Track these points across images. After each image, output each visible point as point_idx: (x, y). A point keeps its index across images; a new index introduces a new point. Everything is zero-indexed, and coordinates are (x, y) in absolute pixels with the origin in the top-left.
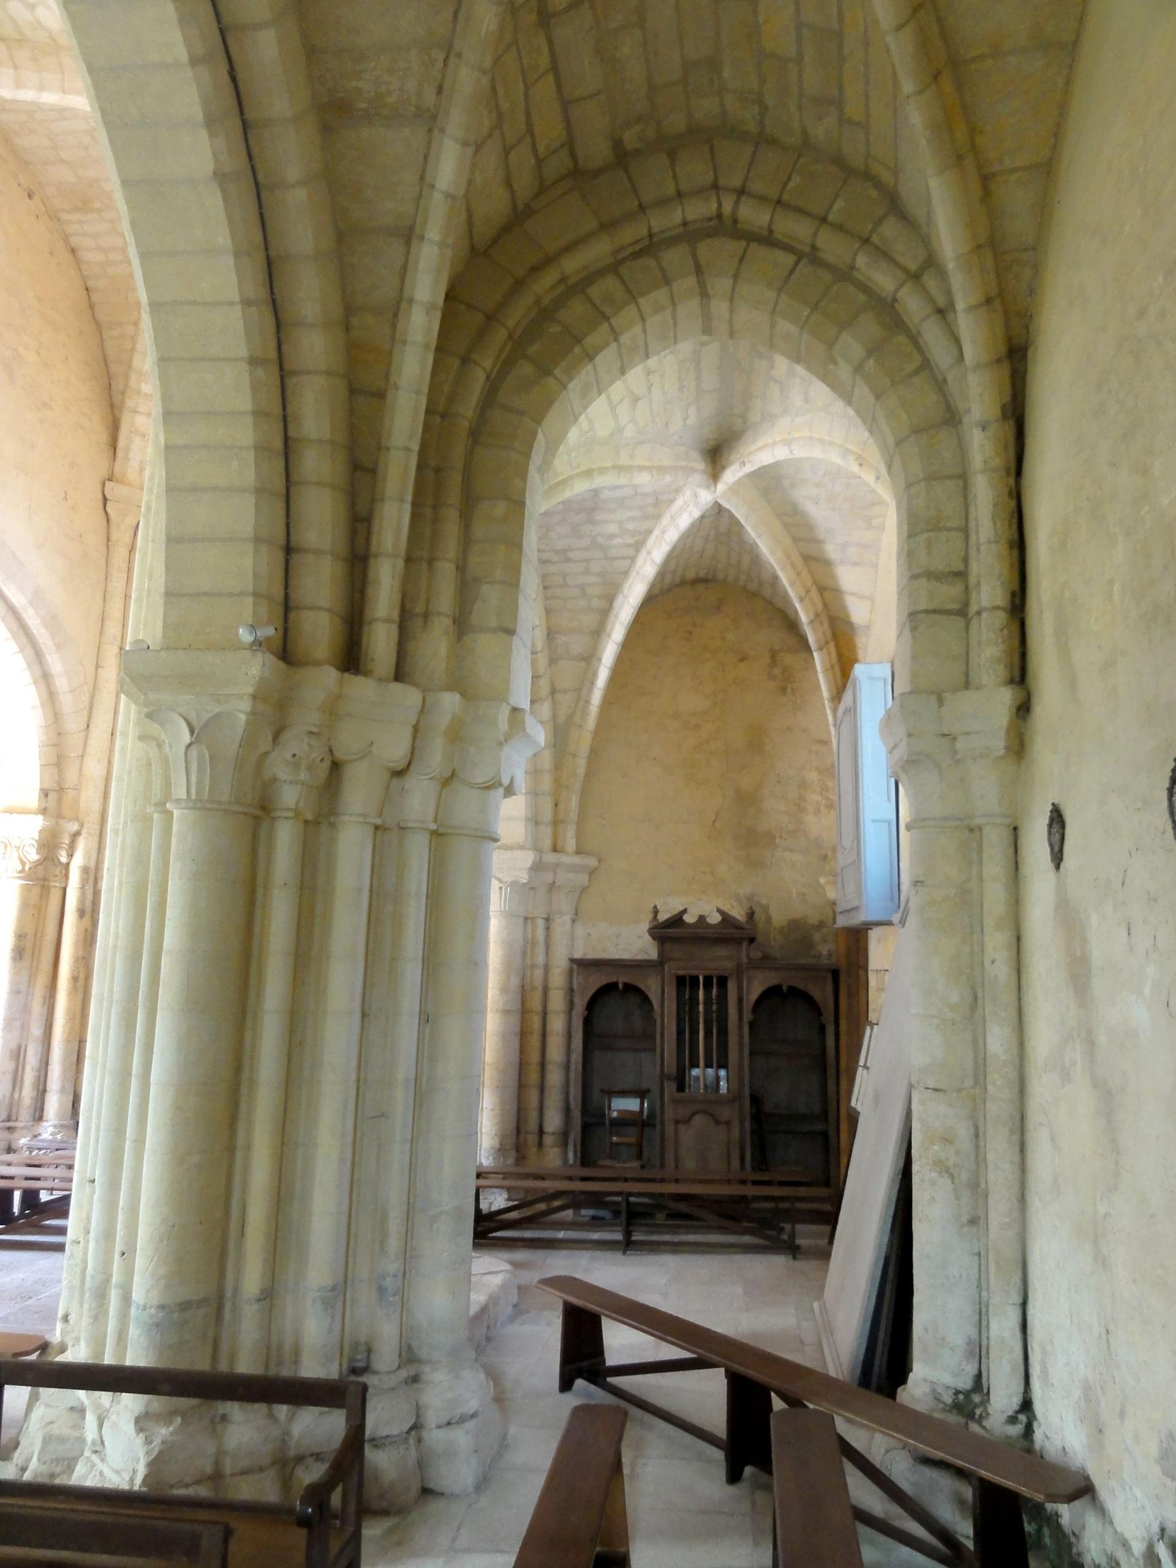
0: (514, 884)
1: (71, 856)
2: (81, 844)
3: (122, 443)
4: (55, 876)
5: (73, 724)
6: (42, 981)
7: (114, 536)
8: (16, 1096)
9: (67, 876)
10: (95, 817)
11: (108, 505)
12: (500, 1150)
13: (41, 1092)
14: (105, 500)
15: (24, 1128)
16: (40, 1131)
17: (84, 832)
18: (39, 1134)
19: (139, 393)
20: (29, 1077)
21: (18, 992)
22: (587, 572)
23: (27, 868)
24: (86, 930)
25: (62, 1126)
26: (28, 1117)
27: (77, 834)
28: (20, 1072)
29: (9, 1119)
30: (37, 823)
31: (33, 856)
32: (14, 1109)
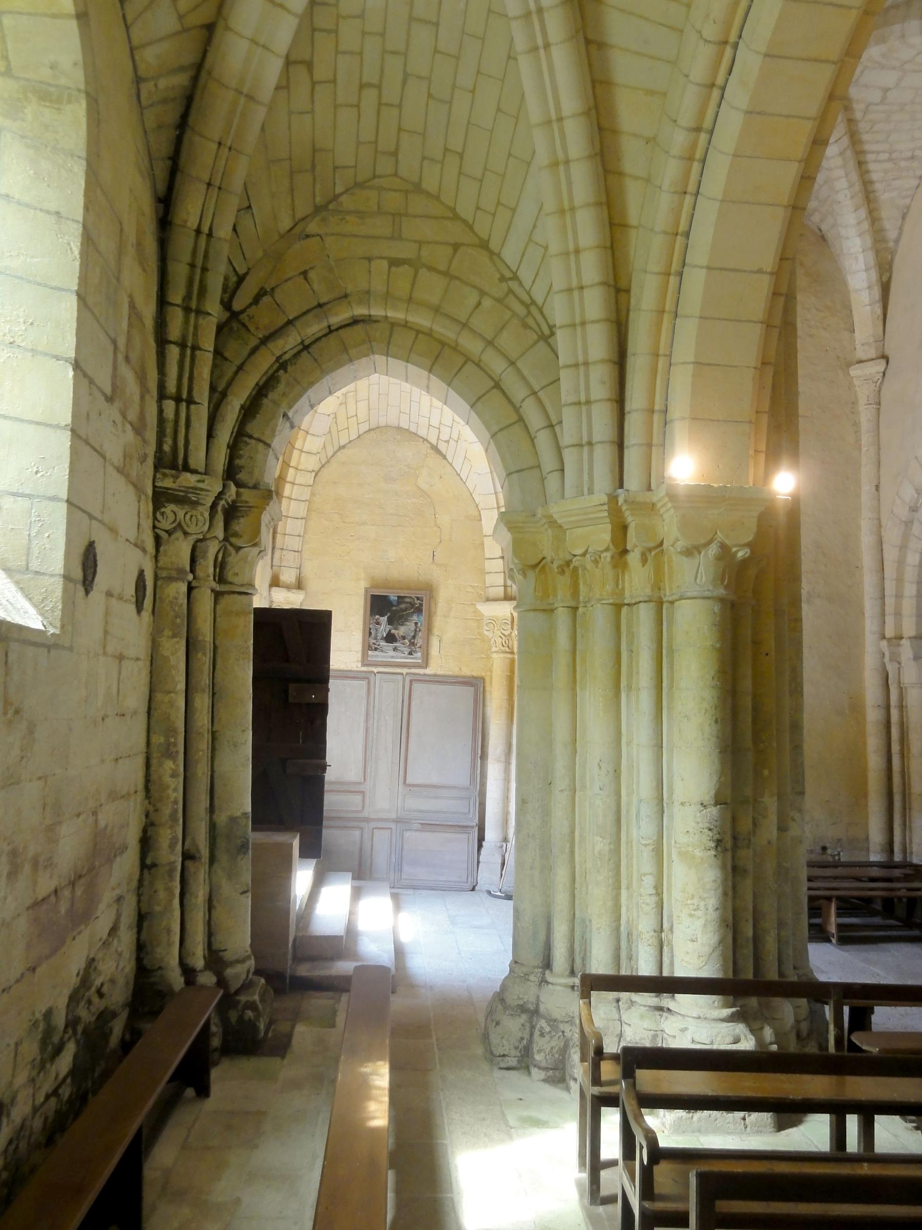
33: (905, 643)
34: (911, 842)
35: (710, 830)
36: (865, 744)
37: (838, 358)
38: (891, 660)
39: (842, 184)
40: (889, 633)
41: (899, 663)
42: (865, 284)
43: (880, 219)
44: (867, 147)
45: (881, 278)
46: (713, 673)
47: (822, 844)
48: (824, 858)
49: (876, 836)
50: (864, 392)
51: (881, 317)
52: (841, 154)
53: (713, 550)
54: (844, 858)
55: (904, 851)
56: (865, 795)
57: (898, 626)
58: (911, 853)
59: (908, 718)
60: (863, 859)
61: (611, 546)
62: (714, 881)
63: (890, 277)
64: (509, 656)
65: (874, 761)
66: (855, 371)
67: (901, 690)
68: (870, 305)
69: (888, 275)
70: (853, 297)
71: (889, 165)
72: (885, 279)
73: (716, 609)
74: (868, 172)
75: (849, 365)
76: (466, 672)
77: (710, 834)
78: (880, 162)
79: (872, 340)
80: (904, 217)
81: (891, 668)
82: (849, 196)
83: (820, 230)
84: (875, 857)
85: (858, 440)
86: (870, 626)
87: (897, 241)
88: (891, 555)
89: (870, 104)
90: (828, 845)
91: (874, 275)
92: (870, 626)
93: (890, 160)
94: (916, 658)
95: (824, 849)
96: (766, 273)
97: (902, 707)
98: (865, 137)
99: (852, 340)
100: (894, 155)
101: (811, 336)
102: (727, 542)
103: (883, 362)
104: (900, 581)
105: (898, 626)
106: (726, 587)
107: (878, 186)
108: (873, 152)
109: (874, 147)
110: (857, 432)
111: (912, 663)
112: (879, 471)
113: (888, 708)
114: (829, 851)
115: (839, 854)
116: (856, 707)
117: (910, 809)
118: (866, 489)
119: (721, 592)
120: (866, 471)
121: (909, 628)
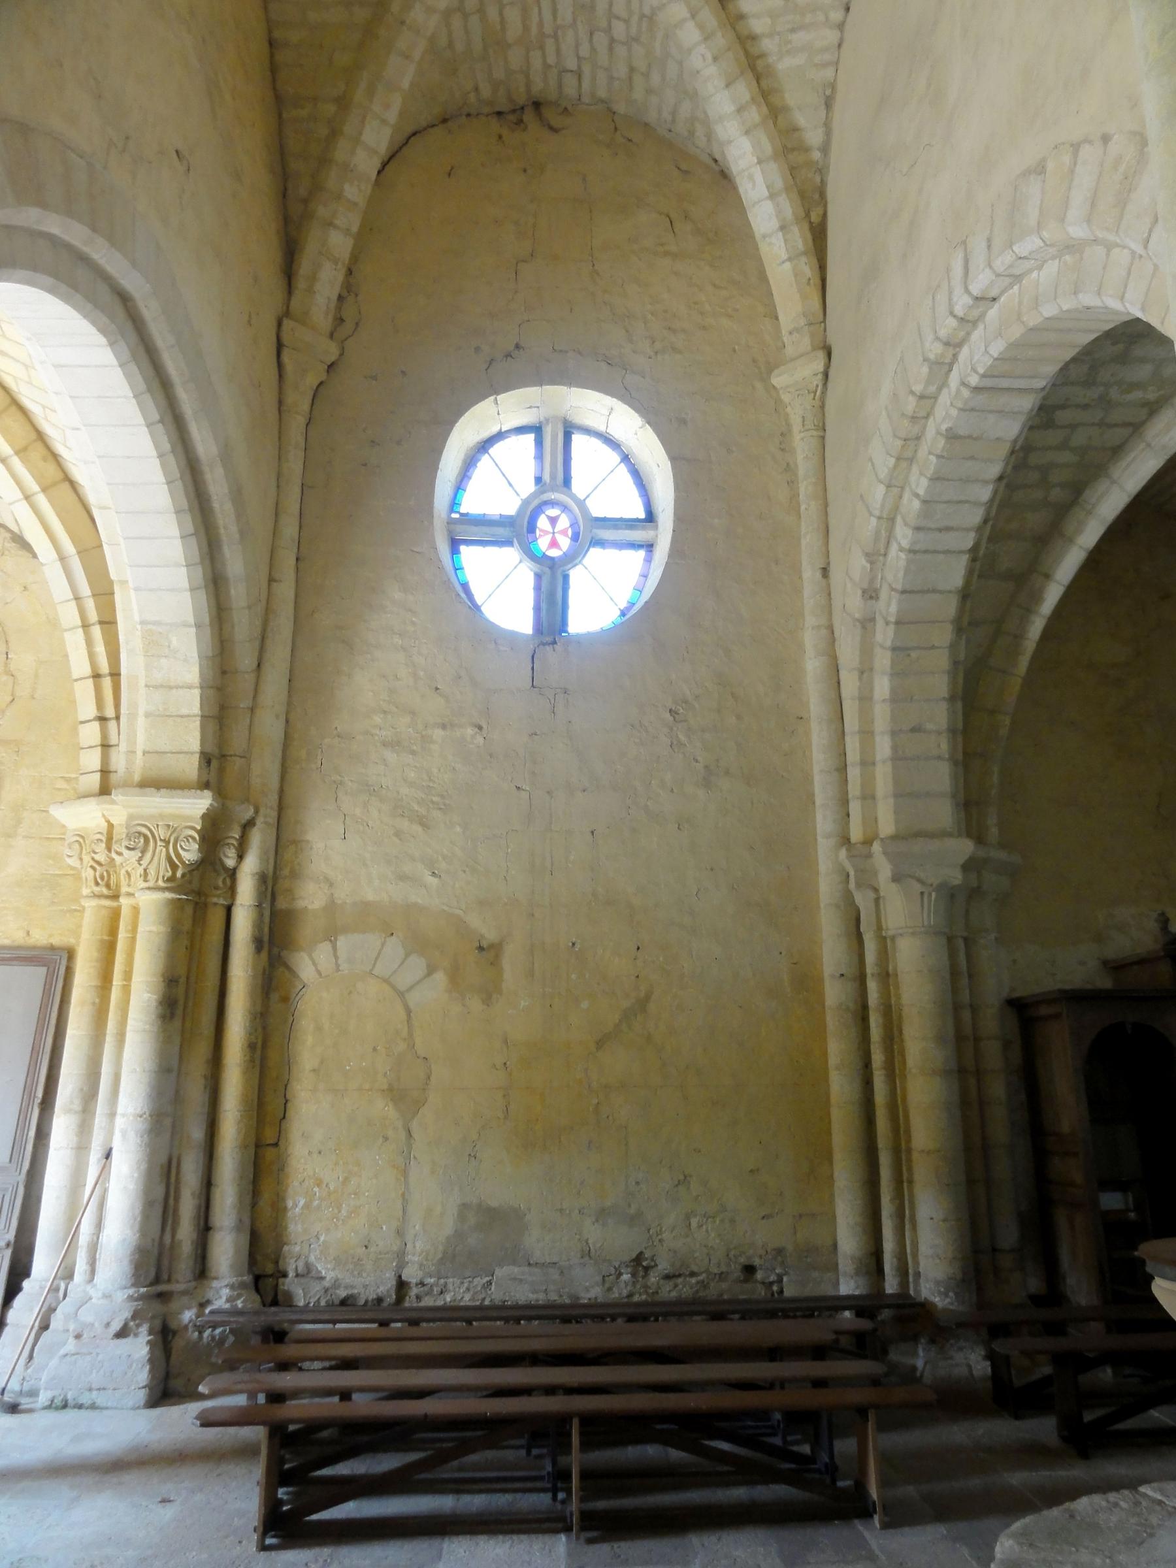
0: (942, 887)
1: (241, 857)
2: (256, 838)
3: (304, 267)
4: (217, 888)
5: (245, 660)
6: (202, 1050)
7: (291, 397)
8: (167, 1239)
9: (232, 890)
10: (273, 799)
12: (963, 1281)
13: (205, 1228)
14: (280, 346)
15: (185, 1293)
16: (210, 1295)
17: (259, 821)
18: (208, 1302)
19: (339, 196)
20: (188, 1207)
21: (169, 1070)
22: (1064, 446)
23: (179, 874)
24: (264, 970)
25: (242, 1286)
26: (189, 1275)
27: (248, 825)
28: (171, 1201)
29: (157, 1280)
30: (199, 804)
31: (191, 853)
32: (165, 1262)
33: (876, 847)
34: (915, 1255)
36: (825, 1054)
37: (754, 361)
38: (859, 885)
39: (690, 34)
40: (856, 834)
41: (876, 890)
42: (774, 224)
43: (785, 109)
45: (808, 215)
49: (849, 1242)
50: (798, 410)
51: (818, 282)
55: (903, 1271)
57: (870, 820)
58: (918, 1275)
59: (899, 997)
60: (826, 1290)
63: (825, 215)
64: (107, 903)
65: (840, 1087)
68: (790, 259)
69: (820, 211)
70: (764, 248)
72: (815, 218)
74: (741, 17)
76: (40, 937)
79: (802, 322)
80: (829, 103)
81: (863, 900)
83: (716, 161)
84: (848, 1287)
85: (794, 496)
86: (824, 822)
87: (825, 149)
88: (850, 685)
90: (757, 1262)
91: (788, 209)
92: (824, 822)
94: (896, 878)
95: (749, 1270)
97: (886, 977)
99: (778, 329)
101: (704, 328)
104: (867, 734)
105: (870, 820)
107: (768, 45)
110: (792, 483)
111: (894, 887)
112: (827, 543)
113: (861, 979)
114: (759, 1275)
115: (780, 1281)
116: (806, 981)
117: (911, 1182)
118: (809, 574)
120: (809, 540)
121: (887, 825)
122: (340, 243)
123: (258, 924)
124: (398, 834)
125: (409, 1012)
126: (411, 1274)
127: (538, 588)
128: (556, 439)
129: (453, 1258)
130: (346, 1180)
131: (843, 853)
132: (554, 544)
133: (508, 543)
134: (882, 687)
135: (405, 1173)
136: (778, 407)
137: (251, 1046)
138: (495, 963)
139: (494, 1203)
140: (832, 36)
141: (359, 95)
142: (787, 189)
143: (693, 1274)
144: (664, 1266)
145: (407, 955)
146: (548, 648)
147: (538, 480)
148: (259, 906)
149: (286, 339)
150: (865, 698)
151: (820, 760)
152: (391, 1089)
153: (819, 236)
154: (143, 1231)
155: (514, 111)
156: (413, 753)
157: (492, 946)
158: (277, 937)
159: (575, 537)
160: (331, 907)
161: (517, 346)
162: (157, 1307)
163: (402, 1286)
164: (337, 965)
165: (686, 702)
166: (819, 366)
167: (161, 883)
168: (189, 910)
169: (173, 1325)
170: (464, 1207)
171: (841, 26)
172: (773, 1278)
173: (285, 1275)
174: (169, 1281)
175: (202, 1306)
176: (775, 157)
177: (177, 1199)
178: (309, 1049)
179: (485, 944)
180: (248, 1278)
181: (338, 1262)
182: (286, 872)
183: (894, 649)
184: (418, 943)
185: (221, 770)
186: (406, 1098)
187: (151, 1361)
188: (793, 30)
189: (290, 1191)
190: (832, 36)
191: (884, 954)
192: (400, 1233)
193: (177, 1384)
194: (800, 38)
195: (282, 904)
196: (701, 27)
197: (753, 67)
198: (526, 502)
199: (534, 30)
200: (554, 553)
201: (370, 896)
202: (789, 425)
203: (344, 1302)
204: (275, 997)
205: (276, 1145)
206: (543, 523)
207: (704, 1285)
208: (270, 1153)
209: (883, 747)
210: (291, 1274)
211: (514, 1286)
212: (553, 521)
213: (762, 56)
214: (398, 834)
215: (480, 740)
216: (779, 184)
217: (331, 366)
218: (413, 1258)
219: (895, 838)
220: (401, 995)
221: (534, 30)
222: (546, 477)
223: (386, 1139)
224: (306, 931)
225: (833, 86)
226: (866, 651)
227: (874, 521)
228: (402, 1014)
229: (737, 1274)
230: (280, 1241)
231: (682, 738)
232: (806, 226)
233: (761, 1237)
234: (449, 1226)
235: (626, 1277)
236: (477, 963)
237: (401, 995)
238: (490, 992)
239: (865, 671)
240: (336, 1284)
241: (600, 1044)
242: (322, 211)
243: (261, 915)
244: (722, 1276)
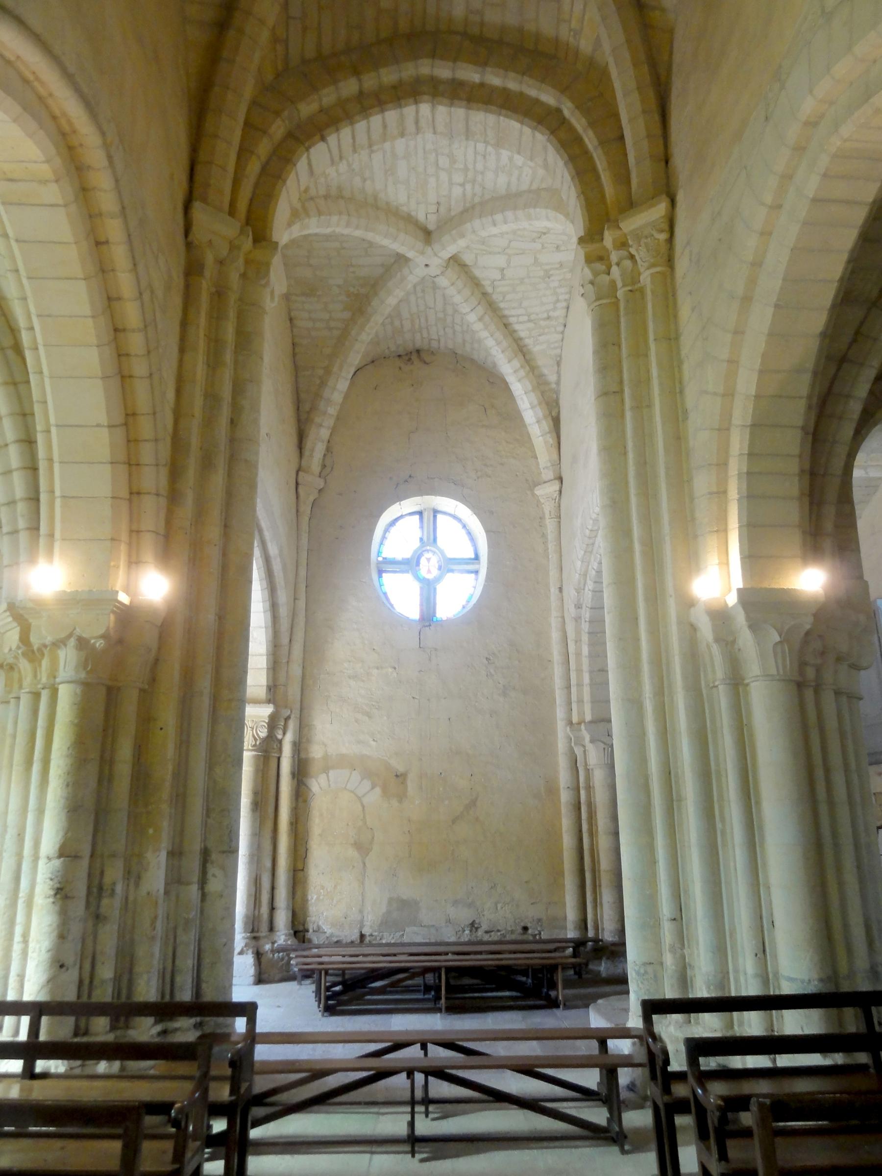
1: (284, 734)
2: (292, 725)
3: (308, 444)
5: (285, 641)
6: (269, 824)
7: (301, 509)
9: (280, 750)
10: (298, 705)
11: (300, 487)
13: (272, 909)
14: (297, 484)
15: (266, 937)
16: (276, 938)
17: (293, 716)
19: (325, 413)
23: (258, 743)
27: (287, 719)
29: (253, 931)
32: (256, 923)
35: (51, 879)
36: (561, 824)
37: (527, 480)
38: (575, 744)
40: (575, 720)
41: (584, 746)
42: (534, 420)
44: (506, 312)
45: (550, 413)
46: (68, 744)
47: (522, 924)
48: (525, 937)
49: (571, 914)
51: (556, 444)
52: (480, 319)
53: (72, 642)
54: (544, 936)
55: (596, 928)
56: (562, 874)
57: (581, 713)
58: (603, 929)
60: (561, 936)
61: (21, 645)
62: (50, 925)
65: (568, 841)
66: (539, 491)
67: (587, 771)
68: (542, 436)
69: (556, 410)
71: (531, 325)
72: (554, 414)
73: (78, 691)
74: (515, 331)
75: (536, 484)
77: (51, 883)
78: (521, 323)
79: (549, 464)
80: (558, 364)
81: (578, 751)
82: (500, 351)
85: (546, 550)
86: (560, 713)
87: (558, 383)
89: (494, 280)
90: (529, 925)
92: (560, 713)
93: (530, 321)
94: (592, 741)
95: (525, 929)
96: (104, 426)
97: (589, 788)
98: (502, 305)
99: (538, 464)
100: (533, 317)
101: (502, 464)
102: (84, 635)
103: (557, 482)
104: (579, 671)
105: (581, 713)
106: (88, 673)
107: (528, 341)
108: (513, 316)
109: (513, 312)
110: (545, 543)
111: (591, 745)
114: (530, 931)
115: (540, 934)
116: (552, 790)
117: (600, 886)
118: (554, 590)
119: (83, 675)
120: (553, 573)
122: (325, 433)
123: (293, 766)
124: (357, 721)
125: (363, 807)
126: (366, 931)
127: (421, 595)
128: (428, 518)
129: (386, 923)
130: (335, 887)
131: (568, 728)
132: (429, 571)
133: (407, 572)
134: (585, 650)
135: (363, 883)
136: (538, 504)
137: (291, 824)
138: (404, 783)
139: (405, 897)
140: (560, 336)
141: (335, 369)
142: (540, 404)
143: (498, 931)
144: (485, 927)
145: (362, 779)
146: (427, 628)
147: (421, 539)
148: (293, 757)
149: (300, 481)
150: (578, 654)
151: (558, 682)
152: (355, 844)
153: (556, 422)
154: (248, 909)
155: (407, 354)
156: (363, 681)
157: (402, 775)
158: (301, 772)
159: (440, 568)
160: (326, 757)
161: (410, 476)
162: (254, 943)
163: (362, 936)
164: (329, 786)
165: (494, 654)
166: (557, 488)
167: (250, 747)
168: (262, 759)
169: (261, 951)
170: (390, 901)
171: (562, 333)
172: (537, 932)
173: (308, 931)
174: (258, 932)
175: (273, 943)
176: (533, 390)
177: (260, 894)
178: (317, 826)
179: (399, 774)
180: (292, 932)
181: (333, 925)
182: (304, 740)
183: (589, 633)
184: (367, 774)
185: (275, 692)
186: (362, 848)
187: (254, 965)
188: (540, 335)
189: (310, 892)
190: (560, 336)
191: (588, 778)
192: (361, 912)
193: (264, 977)
194: (542, 338)
195: (303, 756)
196: (496, 340)
197: (521, 351)
198: (415, 552)
199: (417, 326)
200: (430, 577)
201: (344, 751)
202: (544, 513)
203: (337, 942)
204: (300, 800)
205: (303, 870)
206: (423, 561)
207: (504, 935)
208: (300, 874)
209: (586, 679)
210: (311, 931)
211: (414, 935)
212: (428, 560)
213: (525, 346)
214: (357, 721)
215: (395, 675)
216: (536, 402)
217: (320, 491)
218: (367, 923)
219: (591, 722)
220: (359, 798)
221: (417, 326)
222: (425, 539)
223: (354, 867)
224: (314, 768)
225: (560, 356)
226: (578, 631)
227: (577, 575)
228: (360, 808)
229: (520, 931)
230: (305, 915)
231: (492, 671)
232: (550, 419)
233: (530, 913)
234: (384, 909)
235: (467, 932)
236: (394, 783)
237: (359, 798)
238: (402, 797)
239: (578, 641)
240: (332, 935)
241: (453, 822)
242: (317, 420)
243: (294, 761)
244: (512, 932)
